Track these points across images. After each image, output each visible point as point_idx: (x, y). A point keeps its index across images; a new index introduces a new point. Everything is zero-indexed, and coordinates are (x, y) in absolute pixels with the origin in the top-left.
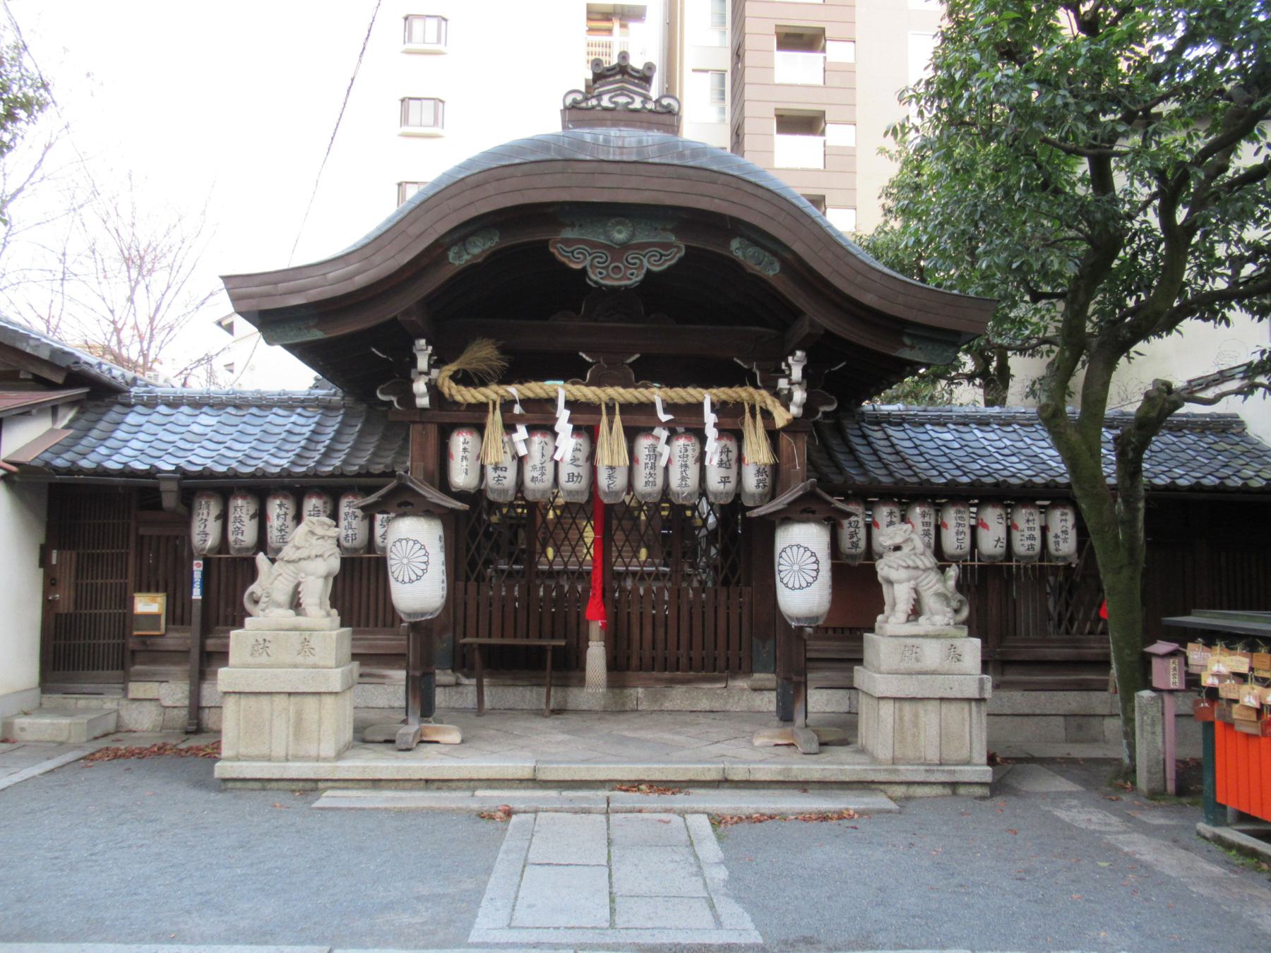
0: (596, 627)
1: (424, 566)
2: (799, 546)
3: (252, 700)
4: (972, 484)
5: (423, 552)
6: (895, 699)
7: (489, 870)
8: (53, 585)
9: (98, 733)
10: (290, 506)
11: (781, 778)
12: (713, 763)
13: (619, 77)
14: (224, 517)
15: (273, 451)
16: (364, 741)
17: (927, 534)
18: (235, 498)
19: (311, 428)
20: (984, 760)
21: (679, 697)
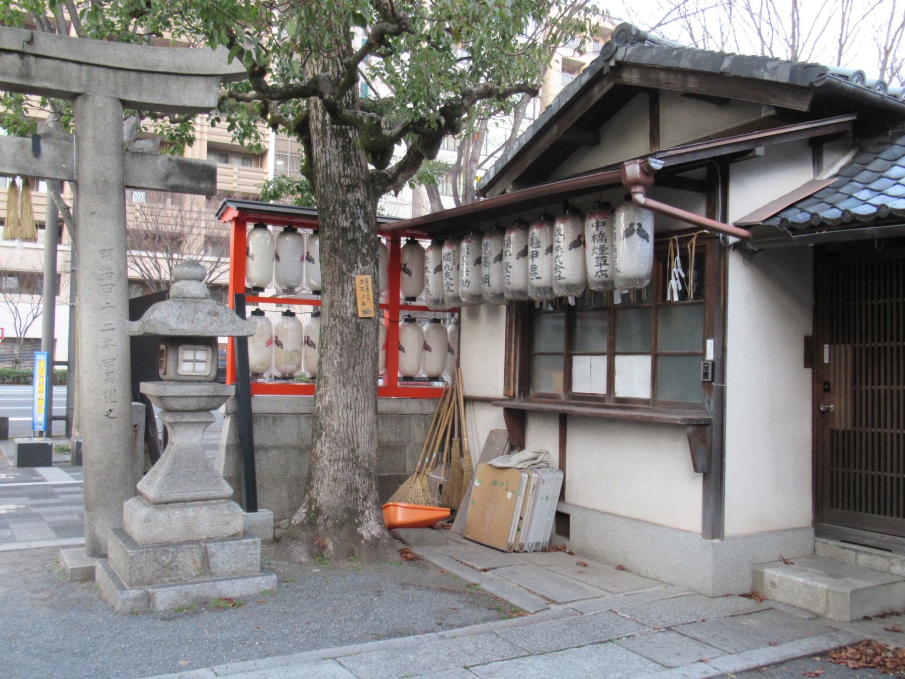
8: (827, 391)
9: (871, 610)
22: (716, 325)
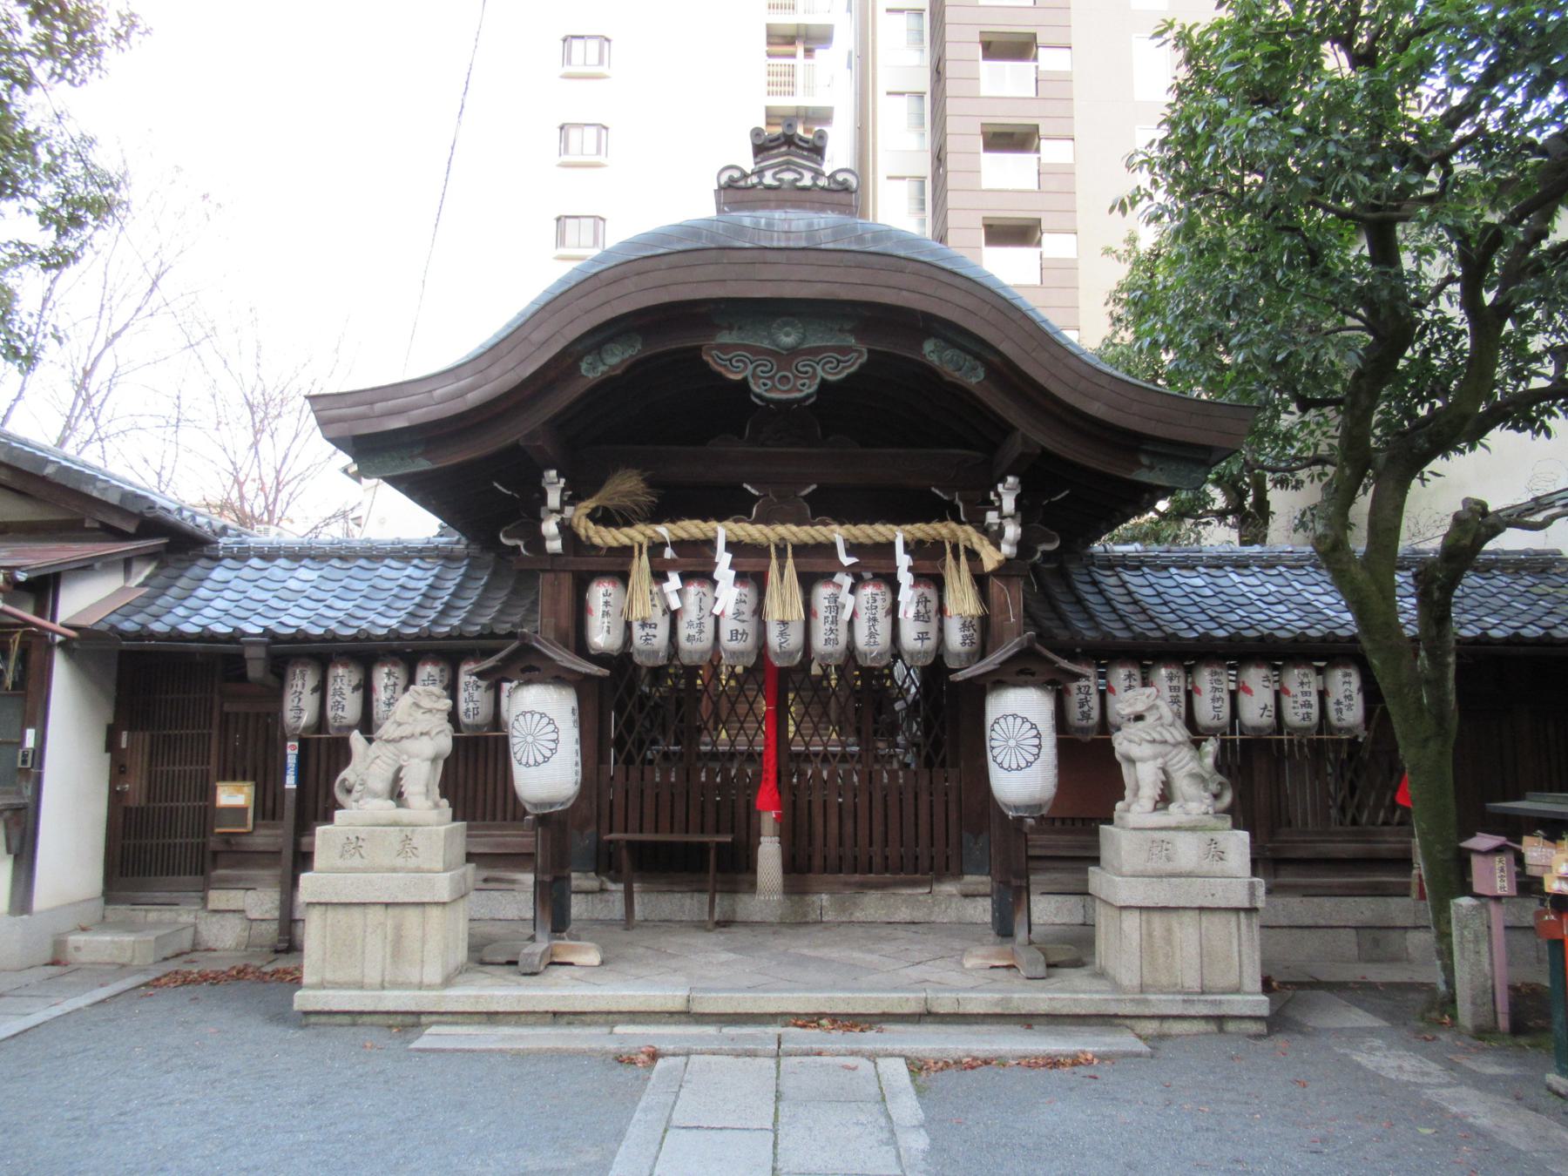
0: (768, 819)
1: (552, 745)
2: (1015, 716)
3: (342, 912)
4: (1229, 639)
5: (551, 727)
6: (1141, 908)
7: (619, 1136)
9: (169, 952)
10: (400, 673)
11: (998, 1010)
12: (914, 991)
13: (784, 149)
14: (321, 689)
15: (381, 609)
16: (483, 963)
17: (1175, 701)
18: (335, 666)
19: (428, 582)
20: (1258, 986)
21: (873, 905)
22: (38, 716)
